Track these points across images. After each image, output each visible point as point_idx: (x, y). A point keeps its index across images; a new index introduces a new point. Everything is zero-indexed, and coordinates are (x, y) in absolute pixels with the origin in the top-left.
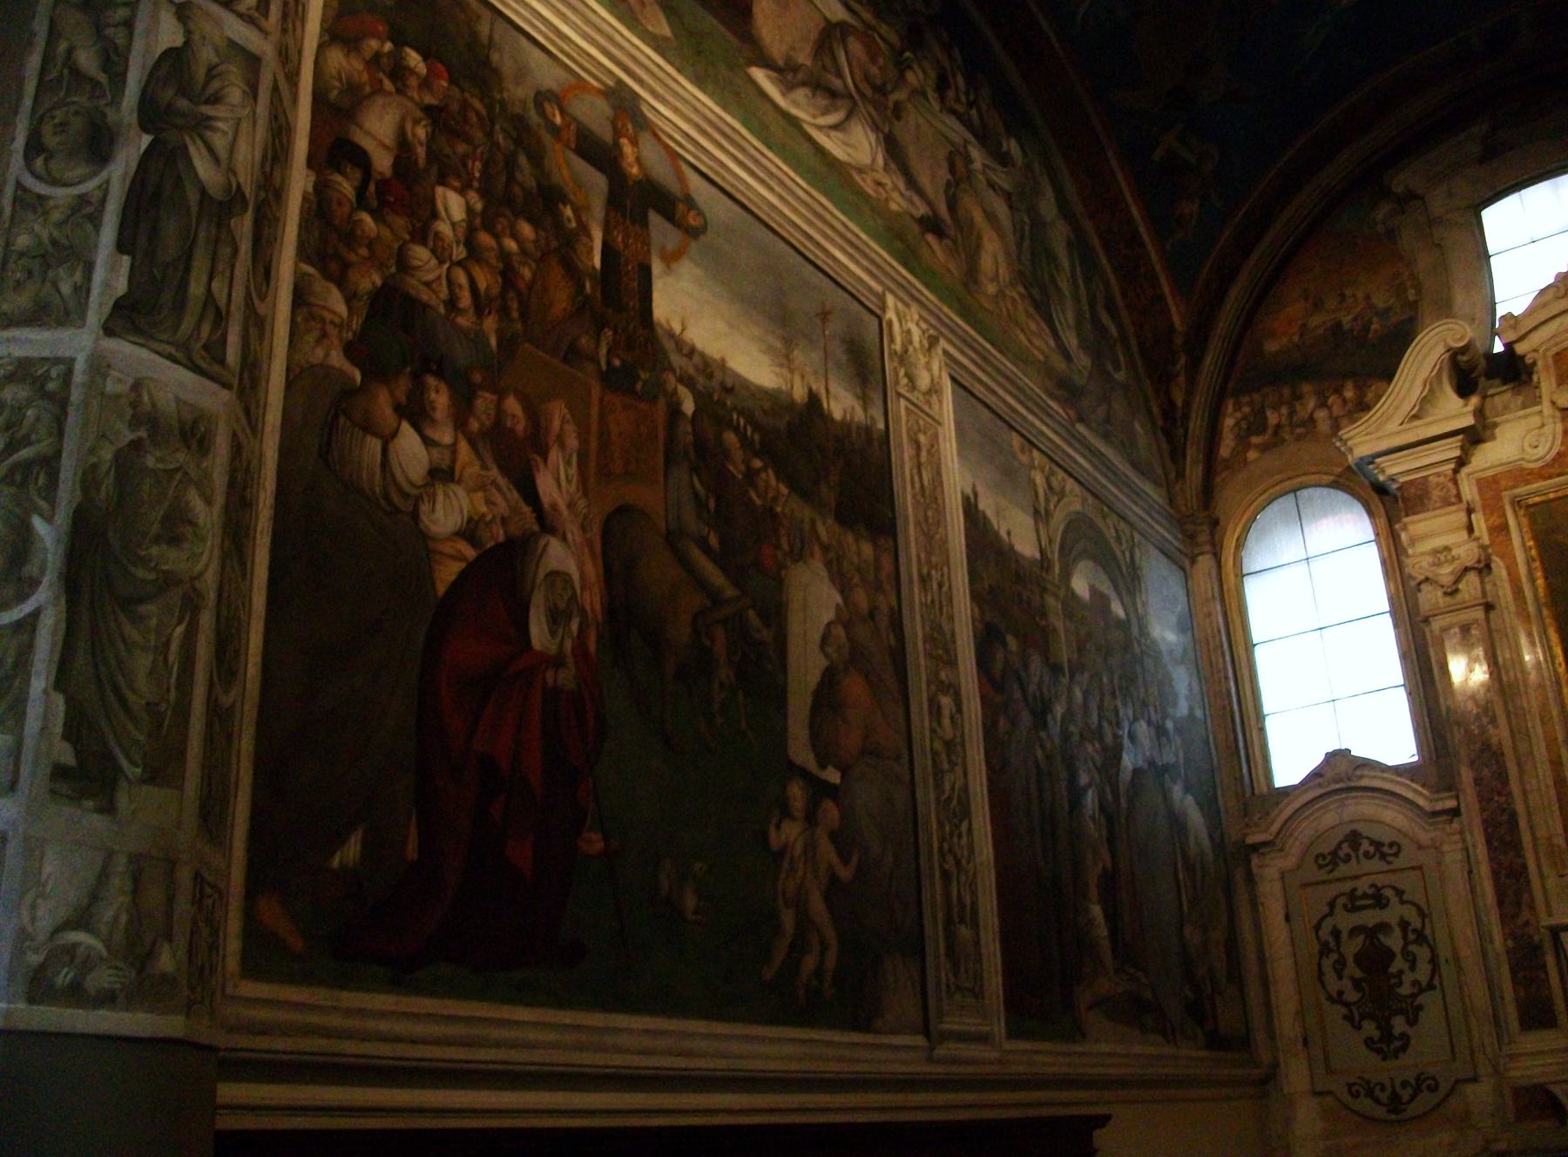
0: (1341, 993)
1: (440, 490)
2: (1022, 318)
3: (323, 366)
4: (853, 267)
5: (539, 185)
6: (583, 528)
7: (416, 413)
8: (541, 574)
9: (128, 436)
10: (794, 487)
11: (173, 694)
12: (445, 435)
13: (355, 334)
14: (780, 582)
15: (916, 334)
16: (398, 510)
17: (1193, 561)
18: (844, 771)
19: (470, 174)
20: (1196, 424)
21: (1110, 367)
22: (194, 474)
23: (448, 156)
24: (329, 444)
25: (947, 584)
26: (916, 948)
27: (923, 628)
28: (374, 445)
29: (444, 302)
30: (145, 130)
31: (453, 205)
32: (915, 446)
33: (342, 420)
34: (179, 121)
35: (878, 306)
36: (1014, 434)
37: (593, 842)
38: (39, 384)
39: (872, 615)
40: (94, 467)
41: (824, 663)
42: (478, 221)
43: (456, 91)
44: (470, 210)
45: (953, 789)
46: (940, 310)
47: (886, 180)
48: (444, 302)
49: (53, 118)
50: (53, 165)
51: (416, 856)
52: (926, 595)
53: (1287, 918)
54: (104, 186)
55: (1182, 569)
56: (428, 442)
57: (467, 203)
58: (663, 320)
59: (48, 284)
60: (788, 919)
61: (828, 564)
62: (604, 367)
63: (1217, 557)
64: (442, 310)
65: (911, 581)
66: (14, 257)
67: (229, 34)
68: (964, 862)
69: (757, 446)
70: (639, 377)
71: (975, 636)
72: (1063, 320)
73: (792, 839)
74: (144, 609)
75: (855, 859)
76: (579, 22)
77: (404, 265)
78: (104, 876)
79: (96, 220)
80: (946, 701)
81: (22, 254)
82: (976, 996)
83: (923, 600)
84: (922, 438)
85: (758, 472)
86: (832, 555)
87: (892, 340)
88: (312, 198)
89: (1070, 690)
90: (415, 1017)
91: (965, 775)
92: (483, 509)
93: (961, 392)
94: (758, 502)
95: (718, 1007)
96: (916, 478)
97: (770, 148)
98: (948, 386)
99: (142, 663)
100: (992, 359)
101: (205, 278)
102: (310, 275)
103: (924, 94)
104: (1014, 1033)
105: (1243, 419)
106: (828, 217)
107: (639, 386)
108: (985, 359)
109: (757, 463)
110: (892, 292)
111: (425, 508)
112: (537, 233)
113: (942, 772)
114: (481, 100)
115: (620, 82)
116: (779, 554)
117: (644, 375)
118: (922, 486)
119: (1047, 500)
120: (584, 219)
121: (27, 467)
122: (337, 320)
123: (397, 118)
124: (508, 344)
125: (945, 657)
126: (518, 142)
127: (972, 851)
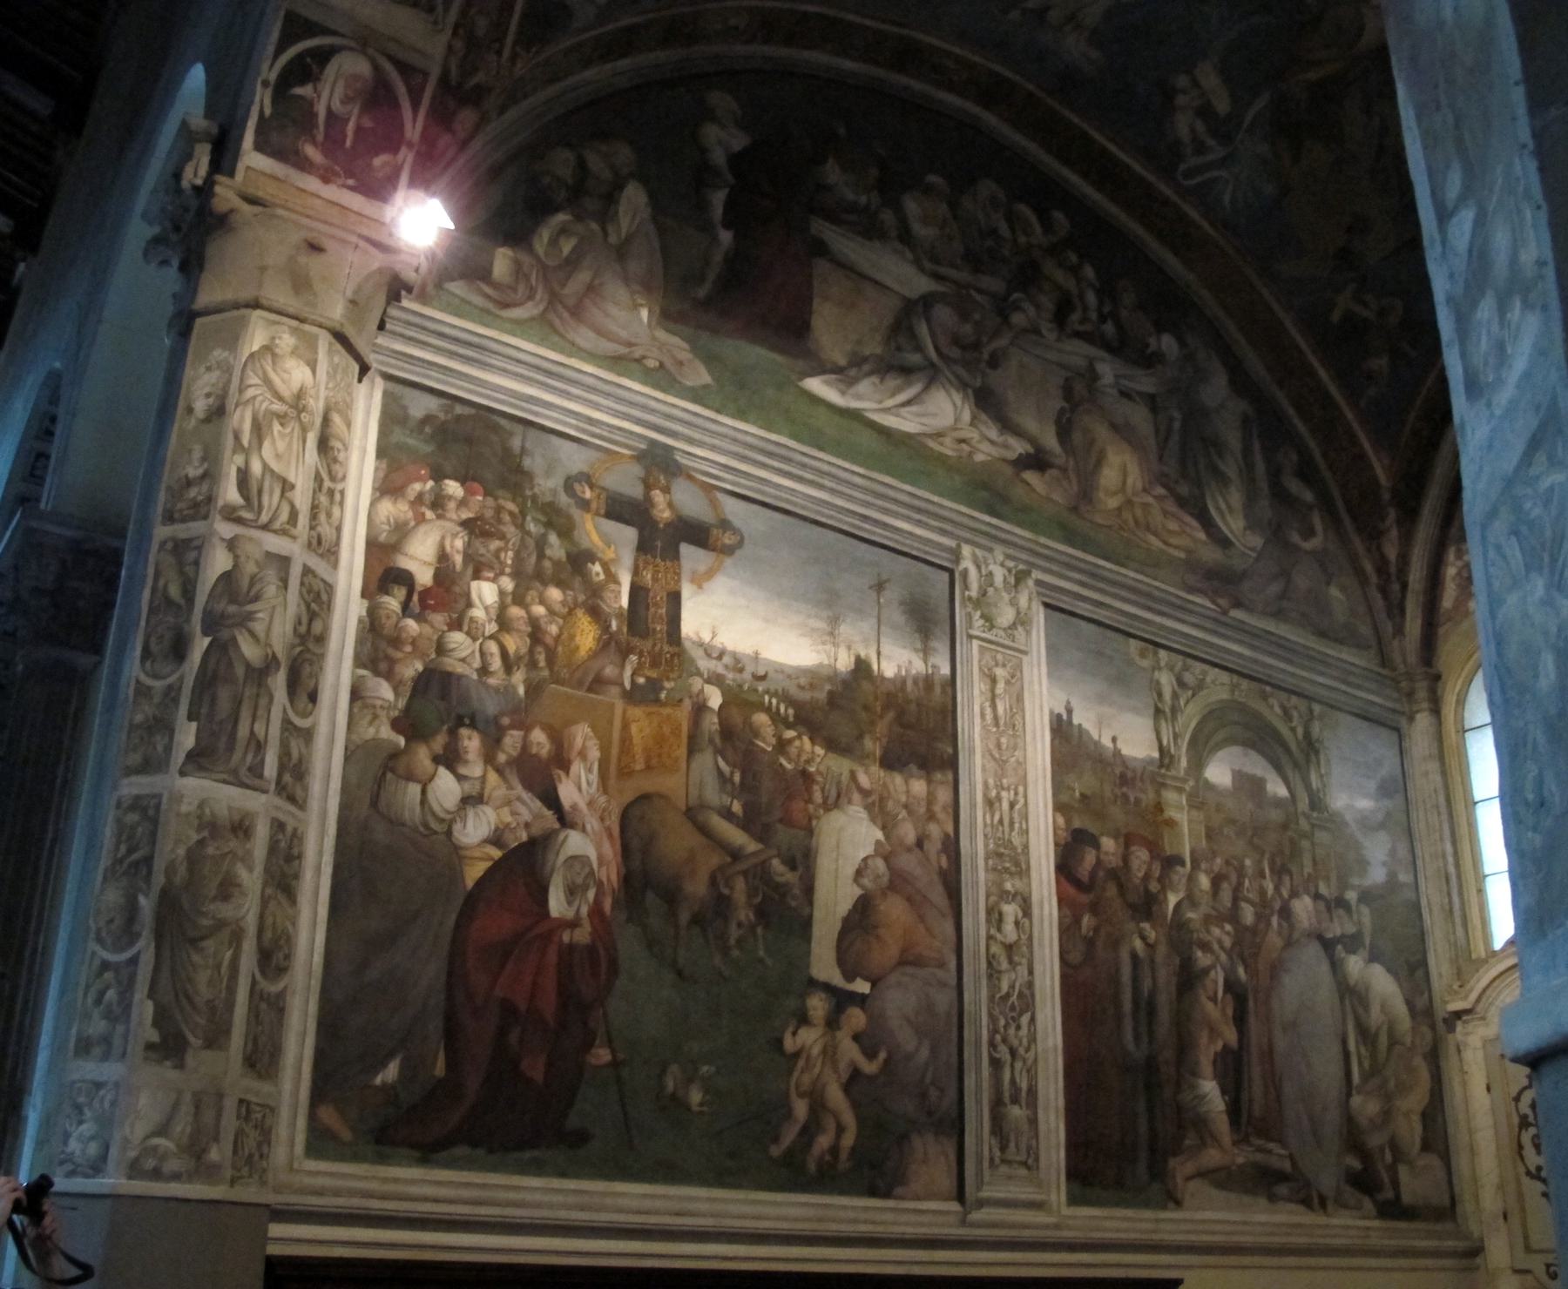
0: (1539, 1169)
1: (471, 813)
2: (1157, 518)
3: (376, 743)
4: (919, 531)
5: (569, 555)
6: (602, 819)
7: (450, 759)
8: (562, 858)
9: (195, 837)
10: (832, 745)
11: (223, 995)
12: (475, 769)
13: (400, 711)
14: (810, 832)
15: (999, 574)
16: (436, 833)
17: (1411, 719)
18: (874, 984)
19: (502, 564)
20: (1416, 575)
21: (1295, 538)
22: (240, 853)
23: (482, 555)
24: (378, 795)
25: (1022, 801)
26: (955, 1126)
27: (986, 845)
28: (414, 789)
29: (477, 670)
30: (205, 633)
31: (485, 593)
32: (988, 681)
33: (389, 775)
34: (230, 622)
35: (951, 561)
36: (1132, 641)
37: (602, 1055)
38: (144, 810)
39: (920, 844)
40: (173, 861)
41: (858, 892)
42: (509, 599)
43: (490, 501)
44: (502, 593)
45: (1012, 987)
46: (1037, 543)
47: (973, 434)
48: (477, 670)
51: (443, 1074)
52: (992, 817)
53: (1488, 1089)
55: (1397, 730)
56: (460, 778)
57: (499, 587)
58: (692, 635)
60: (801, 1109)
61: (868, 808)
62: (627, 685)
63: (1436, 711)
64: (475, 676)
65: (973, 806)
68: (1021, 1051)
69: (791, 719)
70: (662, 688)
71: (1056, 844)
72: (1223, 506)
73: (809, 1042)
74: (204, 944)
75: (882, 1055)
76: (612, 405)
77: (441, 649)
78: (176, 1106)
79: (176, 701)
80: (1010, 910)
82: (1029, 1168)
83: (989, 822)
84: (1000, 672)
85: (790, 741)
86: (874, 797)
87: (966, 587)
88: (367, 619)
89: (1191, 879)
90: (439, 1183)
91: (1031, 972)
92: (509, 819)
93: (1057, 615)
94: (788, 766)
95: (721, 1177)
96: (988, 711)
97: (821, 449)
98: (1039, 616)
99: (202, 978)
100: (1100, 572)
102: (363, 676)
103: (1036, 331)
104: (1073, 1200)
105: (1463, 567)
106: (891, 493)
107: (663, 695)
108: (1093, 575)
109: (790, 734)
110: (967, 541)
111: (457, 827)
112: (564, 593)
113: (1000, 972)
114: (514, 500)
115: (653, 443)
116: (811, 807)
117: (668, 685)
118: (996, 718)
119: (1175, 696)
120: (613, 570)
121: (136, 864)
122: (386, 705)
123: (438, 538)
124: (534, 689)
125: (1013, 869)
126: (549, 525)
127: (1033, 1039)
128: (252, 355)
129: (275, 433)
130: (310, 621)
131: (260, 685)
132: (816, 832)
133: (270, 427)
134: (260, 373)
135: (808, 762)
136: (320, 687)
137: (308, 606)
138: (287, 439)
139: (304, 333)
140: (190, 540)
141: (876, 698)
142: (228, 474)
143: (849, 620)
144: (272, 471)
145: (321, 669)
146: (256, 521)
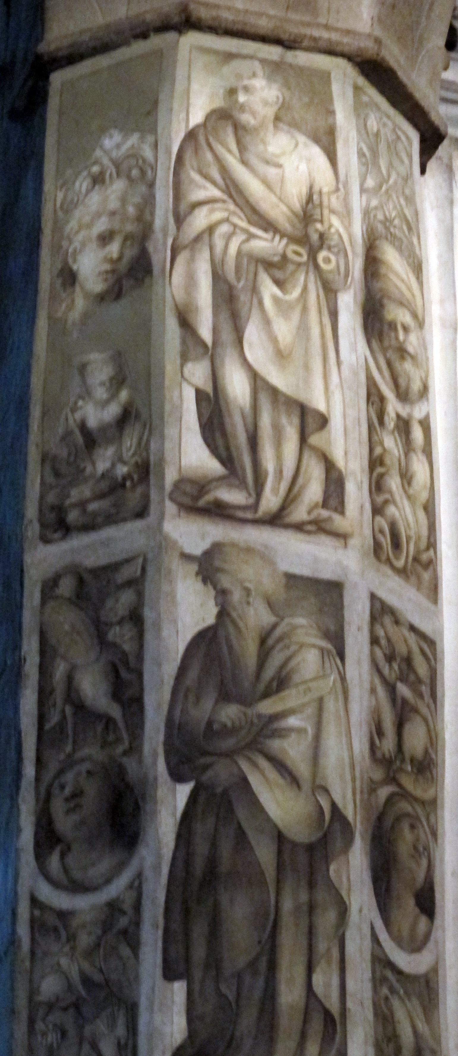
49: (62, 787)
50: (70, 860)
54: (136, 884)
59: (86, 1047)
66: (41, 1012)
67: (285, 566)
81: (50, 1006)
101: (300, 971)
128: (191, 135)
129: (268, 303)
130: (400, 726)
131: (311, 885)
133: (255, 290)
134: (217, 176)
136: (437, 880)
137: (391, 690)
138: (296, 316)
139: (301, 71)
140: (115, 567)
142: (178, 408)
144: (274, 392)
145: (434, 834)
146: (255, 507)
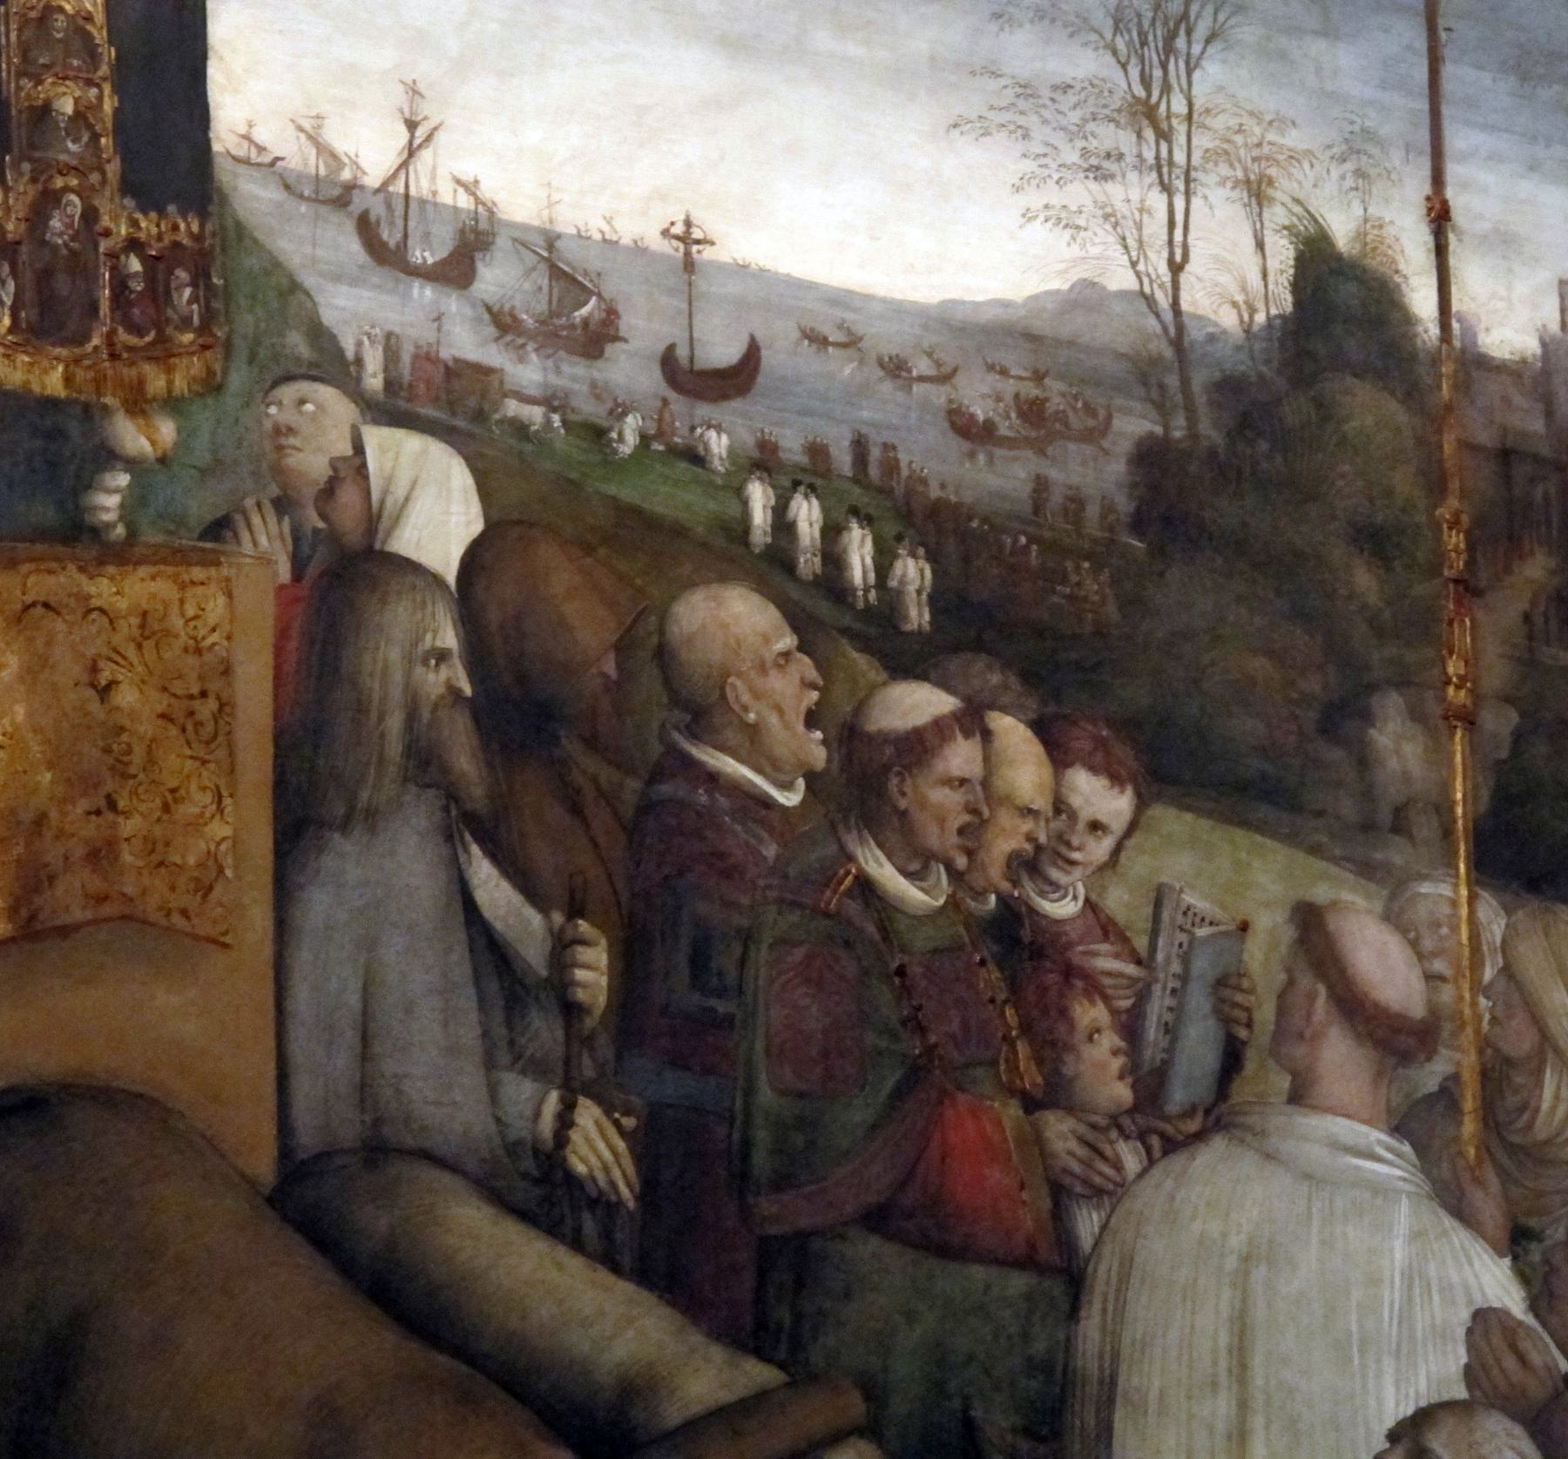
69: (917, 616)
116: (1060, 1131)
117: (131, 437)
132: (1103, 1274)
135: (1029, 864)
141: (1437, 486)
143: (1246, 32)
